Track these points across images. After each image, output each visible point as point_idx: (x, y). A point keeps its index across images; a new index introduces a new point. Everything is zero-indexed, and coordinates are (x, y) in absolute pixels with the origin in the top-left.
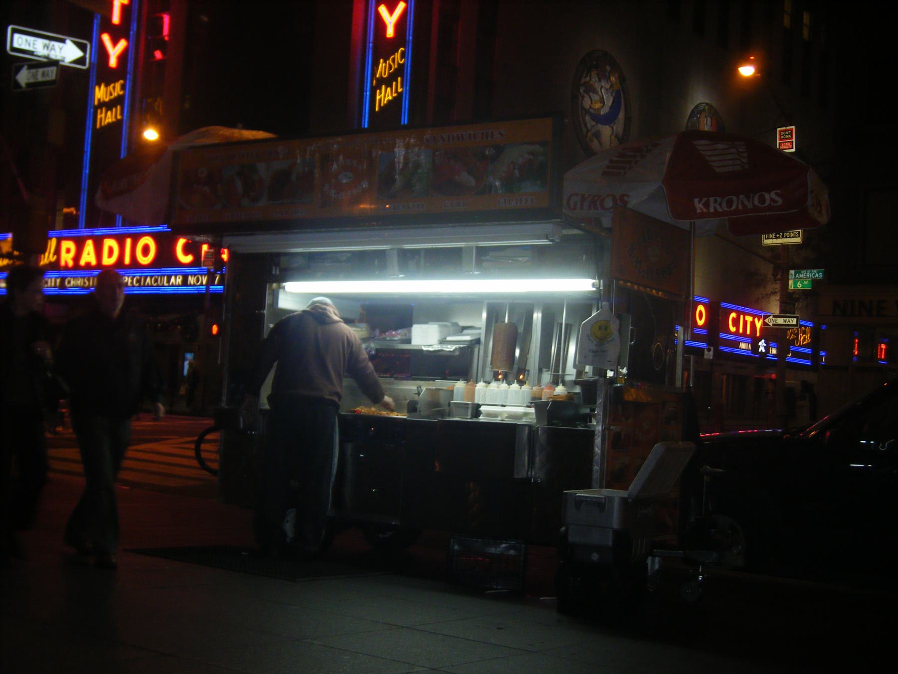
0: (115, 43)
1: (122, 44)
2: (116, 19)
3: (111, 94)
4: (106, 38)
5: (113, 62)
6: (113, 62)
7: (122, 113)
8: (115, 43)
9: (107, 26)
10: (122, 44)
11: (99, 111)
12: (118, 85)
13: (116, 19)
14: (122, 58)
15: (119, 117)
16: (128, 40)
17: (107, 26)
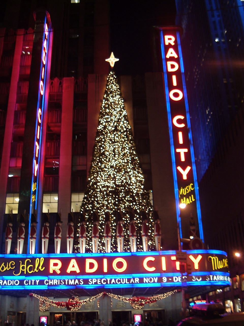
0: (184, 169)
1: (188, 168)
2: (183, 159)
3: (187, 191)
4: (179, 168)
5: (185, 178)
6: (185, 178)
7: (195, 198)
8: (184, 169)
9: (179, 163)
10: (188, 168)
11: (182, 200)
12: (190, 187)
13: (183, 159)
14: (190, 174)
15: (193, 200)
16: (191, 166)
17: (179, 163)
